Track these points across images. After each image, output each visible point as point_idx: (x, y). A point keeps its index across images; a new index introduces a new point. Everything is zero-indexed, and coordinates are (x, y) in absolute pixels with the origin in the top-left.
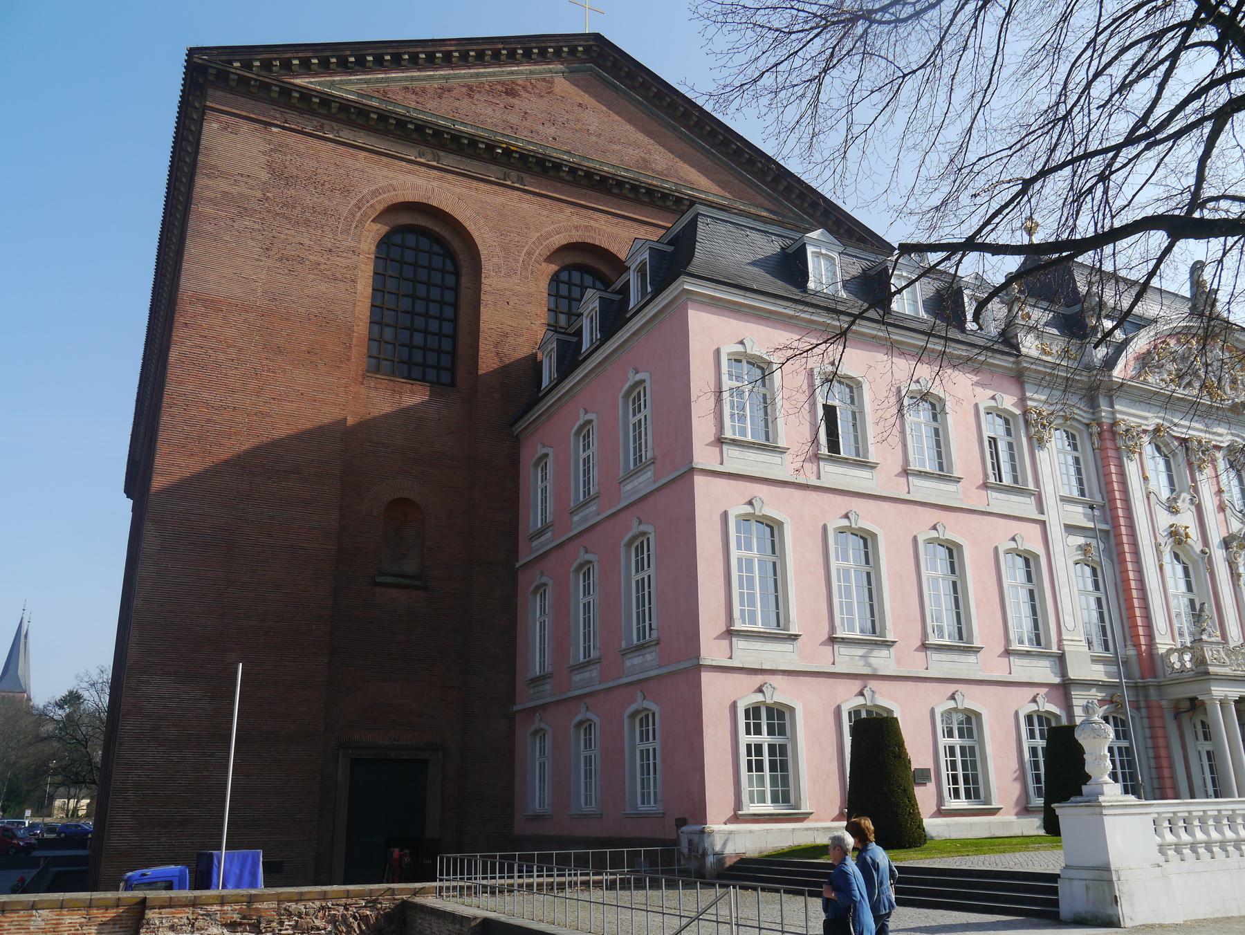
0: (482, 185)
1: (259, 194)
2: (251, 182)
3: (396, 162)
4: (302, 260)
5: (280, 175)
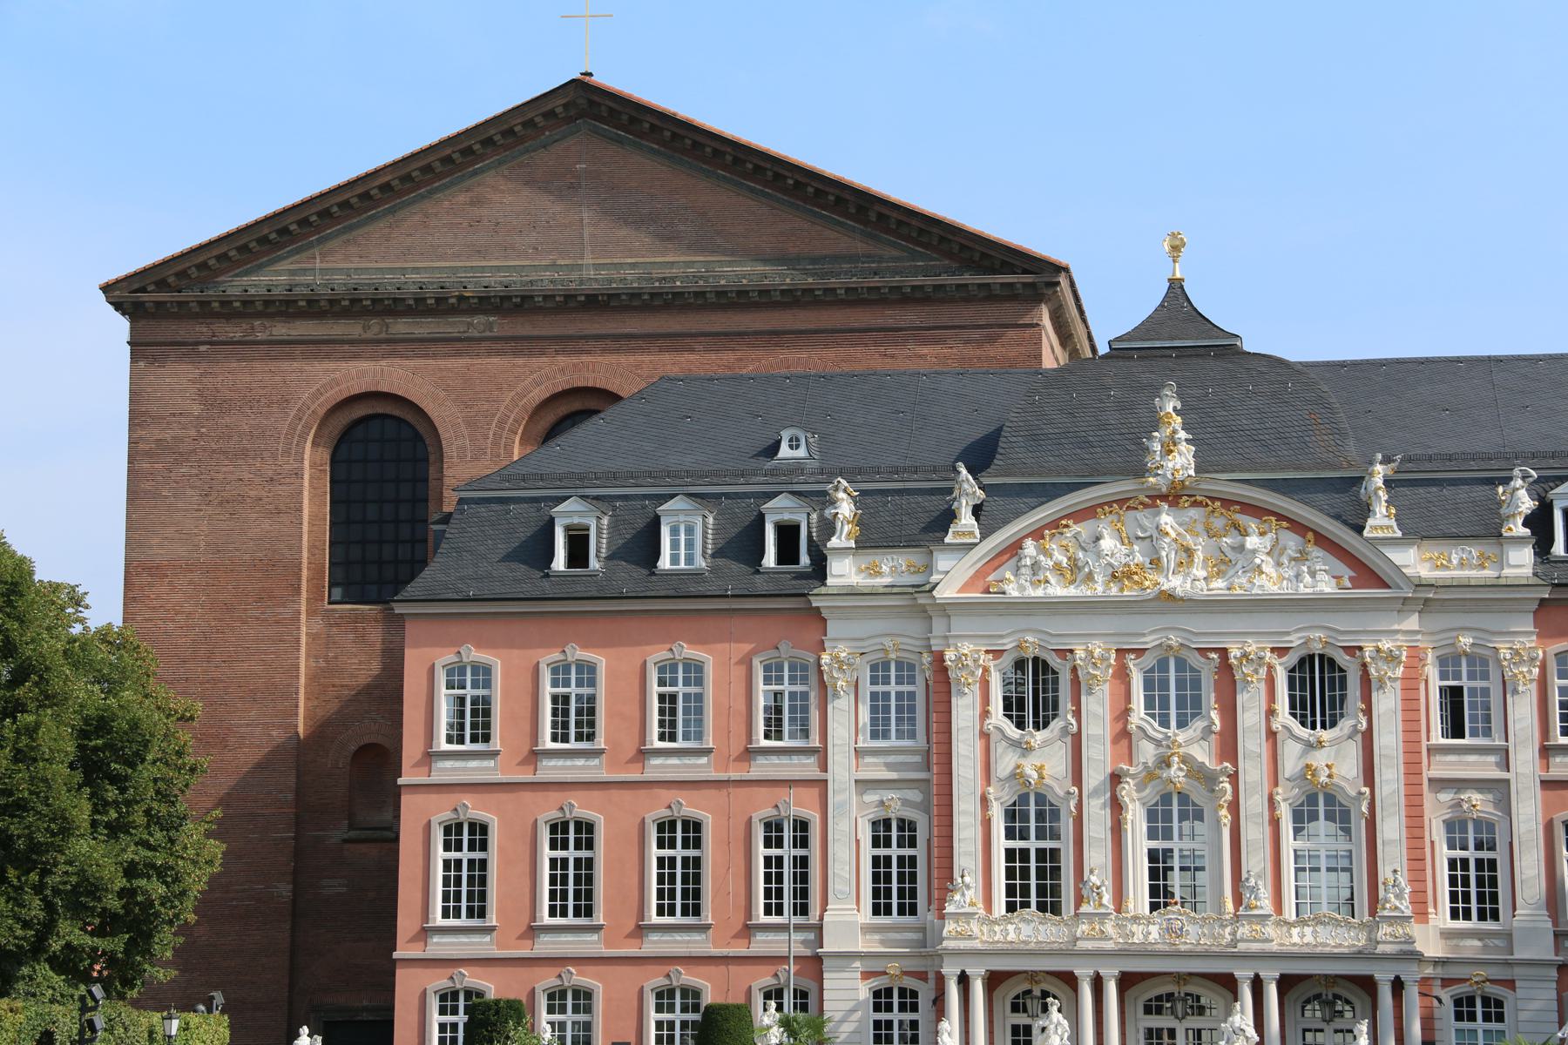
1: (193, 433)
2: (183, 420)
3: (337, 347)
5: (214, 403)
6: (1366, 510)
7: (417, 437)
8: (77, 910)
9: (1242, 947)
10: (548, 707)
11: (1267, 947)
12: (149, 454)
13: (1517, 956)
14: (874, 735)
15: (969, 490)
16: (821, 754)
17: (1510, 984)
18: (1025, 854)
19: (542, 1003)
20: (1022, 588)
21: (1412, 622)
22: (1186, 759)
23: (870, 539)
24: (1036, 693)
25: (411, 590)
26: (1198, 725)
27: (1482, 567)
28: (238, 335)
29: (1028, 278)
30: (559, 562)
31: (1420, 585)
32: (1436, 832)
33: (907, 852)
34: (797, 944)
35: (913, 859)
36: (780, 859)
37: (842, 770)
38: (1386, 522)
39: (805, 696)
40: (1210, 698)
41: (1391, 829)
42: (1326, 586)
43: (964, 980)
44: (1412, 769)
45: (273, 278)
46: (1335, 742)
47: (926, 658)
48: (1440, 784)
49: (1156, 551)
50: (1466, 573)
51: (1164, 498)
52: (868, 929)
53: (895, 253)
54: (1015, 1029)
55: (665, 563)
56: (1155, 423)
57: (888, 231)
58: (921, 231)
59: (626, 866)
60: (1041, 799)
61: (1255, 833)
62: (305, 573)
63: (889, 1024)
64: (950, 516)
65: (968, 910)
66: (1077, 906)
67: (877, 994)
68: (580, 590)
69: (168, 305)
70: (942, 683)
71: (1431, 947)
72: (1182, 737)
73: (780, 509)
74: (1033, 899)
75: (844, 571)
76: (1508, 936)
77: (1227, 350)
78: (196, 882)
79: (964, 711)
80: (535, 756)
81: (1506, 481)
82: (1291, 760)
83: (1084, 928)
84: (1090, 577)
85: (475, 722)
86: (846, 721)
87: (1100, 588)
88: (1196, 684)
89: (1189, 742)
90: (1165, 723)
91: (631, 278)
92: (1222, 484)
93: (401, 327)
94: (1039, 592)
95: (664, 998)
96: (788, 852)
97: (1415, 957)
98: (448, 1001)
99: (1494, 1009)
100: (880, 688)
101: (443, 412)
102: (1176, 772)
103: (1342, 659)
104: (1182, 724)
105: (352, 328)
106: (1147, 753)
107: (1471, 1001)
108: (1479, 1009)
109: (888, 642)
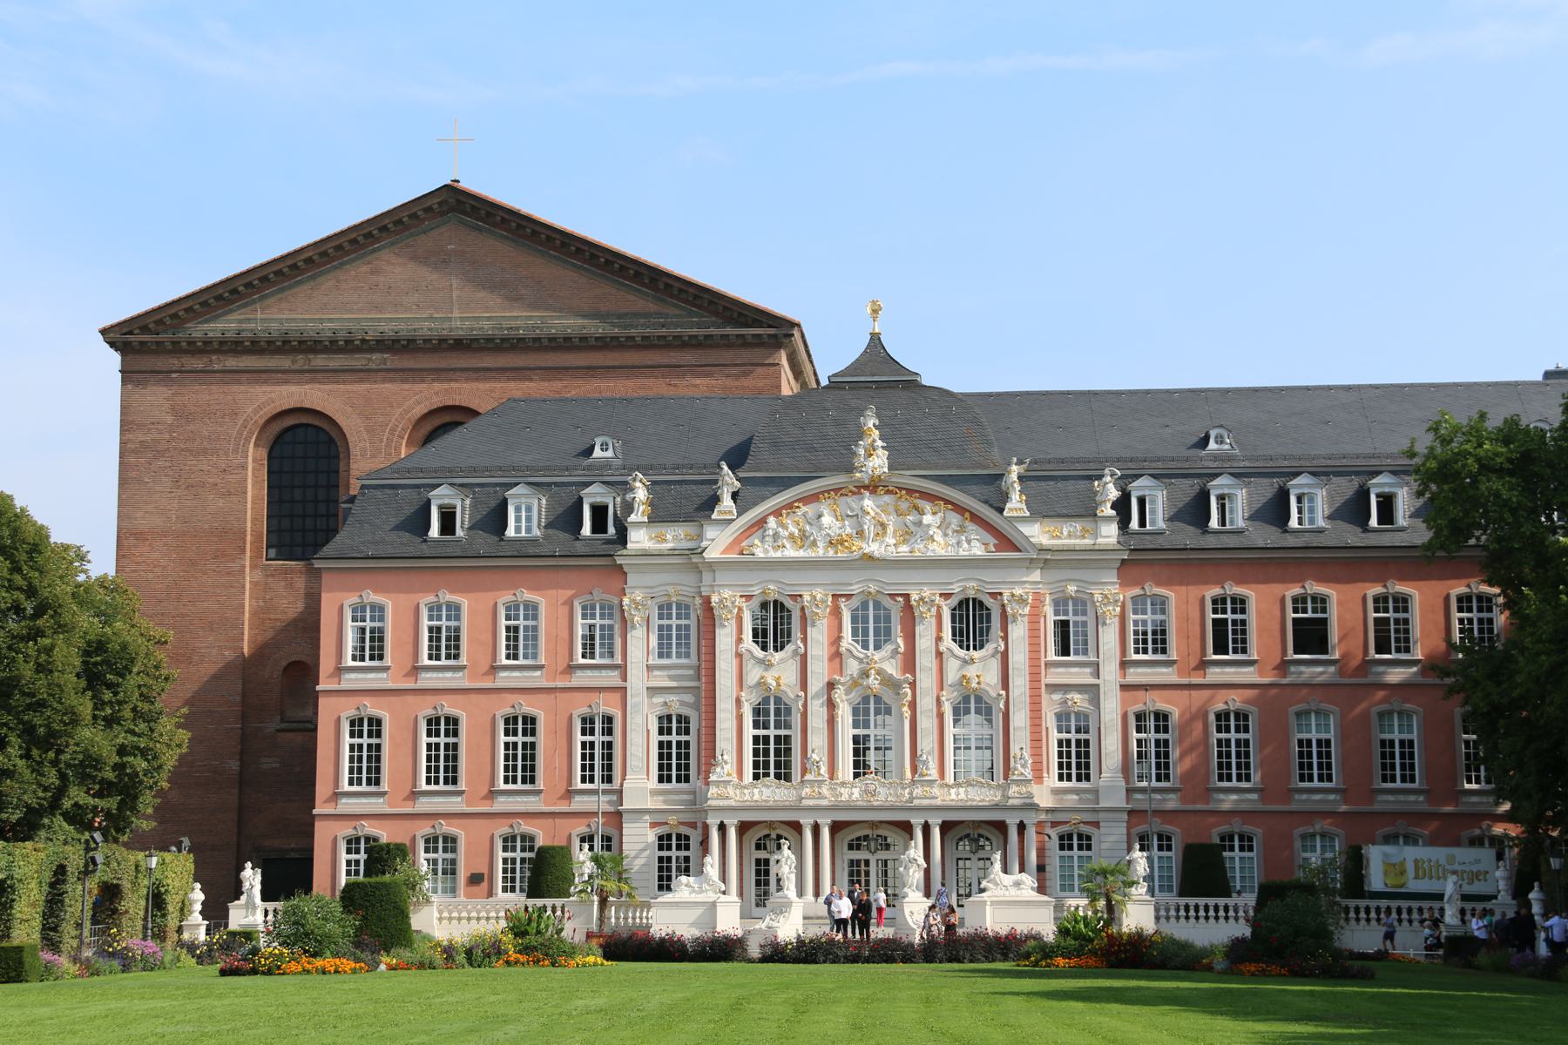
0: (348, 377)
1: (167, 436)
4: (203, 484)
5: (182, 414)
6: (1005, 497)
7: (331, 441)
8: (84, 778)
9: (916, 802)
10: (425, 635)
11: (933, 802)
12: (134, 451)
13: (1101, 805)
14: (661, 655)
15: (729, 481)
16: (623, 669)
17: (1096, 824)
18: (766, 739)
19: (421, 845)
20: (766, 551)
21: (1036, 576)
22: (879, 672)
23: (660, 515)
24: (776, 625)
25: (327, 550)
26: (889, 648)
27: (1083, 537)
28: (200, 366)
29: (772, 331)
30: (434, 531)
31: (1042, 550)
32: (1050, 721)
33: (683, 738)
34: (604, 803)
35: (687, 743)
36: (592, 744)
37: (637, 680)
38: (1019, 505)
39: (611, 627)
40: (897, 629)
41: (1020, 719)
42: (978, 550)
43: (722, 828)
44: (1035, 677)
45: (226, 325)
46: (982, 659)
47: (698, 601)
48: (1053, 688)
49: (861, 525)
50: (1073, 541)
51: (866, 487)
52: (654, 793)
53: (677, 312)
54: (758, 862)
55: (511, 532)
56: (861, 435)
57: (671, 296)
58: (696, 297)
59: (482, 749)
60: (778, 700)
61: (926, 723)
62: (249, 538)
63: (669, 859)
64: (715, 500)
65: (726, 778)
66: (803, 775)
67: (661, 838)
68: (449, 551)
69: (151, 344)
70: (709, 618)
71: (1044, 799)
72: (877, 656)
73: (594, 494)
74: (772, 771)
75: (639, 539)
76: (1096, 792)
77: (910, 384)
78: (170, 759)
79: (725, 639)
80: (416, 670)
81: (1100, 477)
82: (953, 671)
83: (807, 790)
84: (814, 544)
85: (373, 646)
86: (640, 646)
87: (821, 552)
88: (888, 619)
89: (882, 660)
90: (865, 646)
91: (486, 327)
92: (907, 478)
93: (320, 361)
94: (778, 554)
95: (509, 842)
96: (598, 738)
97: (1033, 807)
98: (353, 844)
99: (1086, 842)
100: (665, 622)
101: (349, 422)
102: (873, 682)
103: (988, 601)
104: (877, 647)
105: (284, 362)
106: (853, 667)
107: (1070, 837)
108: (1075, 842)
109: (671, 590)
